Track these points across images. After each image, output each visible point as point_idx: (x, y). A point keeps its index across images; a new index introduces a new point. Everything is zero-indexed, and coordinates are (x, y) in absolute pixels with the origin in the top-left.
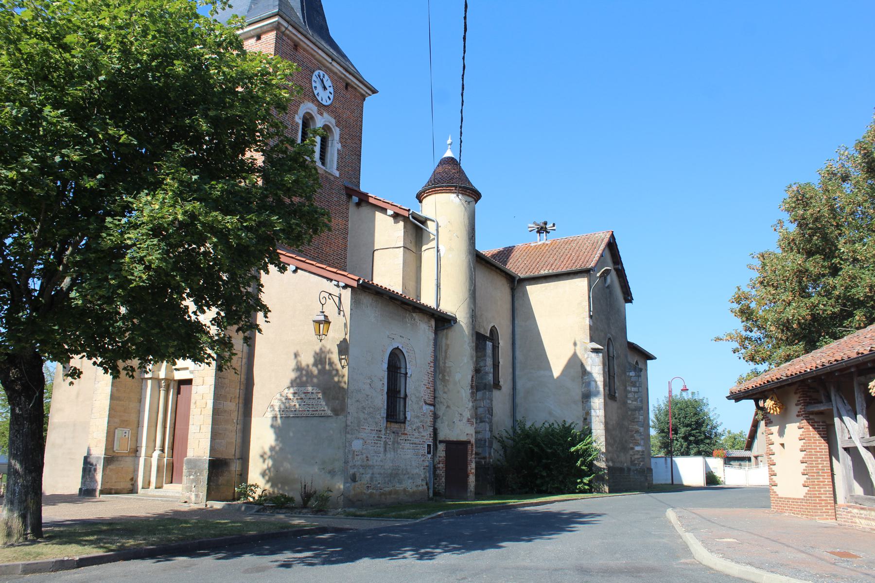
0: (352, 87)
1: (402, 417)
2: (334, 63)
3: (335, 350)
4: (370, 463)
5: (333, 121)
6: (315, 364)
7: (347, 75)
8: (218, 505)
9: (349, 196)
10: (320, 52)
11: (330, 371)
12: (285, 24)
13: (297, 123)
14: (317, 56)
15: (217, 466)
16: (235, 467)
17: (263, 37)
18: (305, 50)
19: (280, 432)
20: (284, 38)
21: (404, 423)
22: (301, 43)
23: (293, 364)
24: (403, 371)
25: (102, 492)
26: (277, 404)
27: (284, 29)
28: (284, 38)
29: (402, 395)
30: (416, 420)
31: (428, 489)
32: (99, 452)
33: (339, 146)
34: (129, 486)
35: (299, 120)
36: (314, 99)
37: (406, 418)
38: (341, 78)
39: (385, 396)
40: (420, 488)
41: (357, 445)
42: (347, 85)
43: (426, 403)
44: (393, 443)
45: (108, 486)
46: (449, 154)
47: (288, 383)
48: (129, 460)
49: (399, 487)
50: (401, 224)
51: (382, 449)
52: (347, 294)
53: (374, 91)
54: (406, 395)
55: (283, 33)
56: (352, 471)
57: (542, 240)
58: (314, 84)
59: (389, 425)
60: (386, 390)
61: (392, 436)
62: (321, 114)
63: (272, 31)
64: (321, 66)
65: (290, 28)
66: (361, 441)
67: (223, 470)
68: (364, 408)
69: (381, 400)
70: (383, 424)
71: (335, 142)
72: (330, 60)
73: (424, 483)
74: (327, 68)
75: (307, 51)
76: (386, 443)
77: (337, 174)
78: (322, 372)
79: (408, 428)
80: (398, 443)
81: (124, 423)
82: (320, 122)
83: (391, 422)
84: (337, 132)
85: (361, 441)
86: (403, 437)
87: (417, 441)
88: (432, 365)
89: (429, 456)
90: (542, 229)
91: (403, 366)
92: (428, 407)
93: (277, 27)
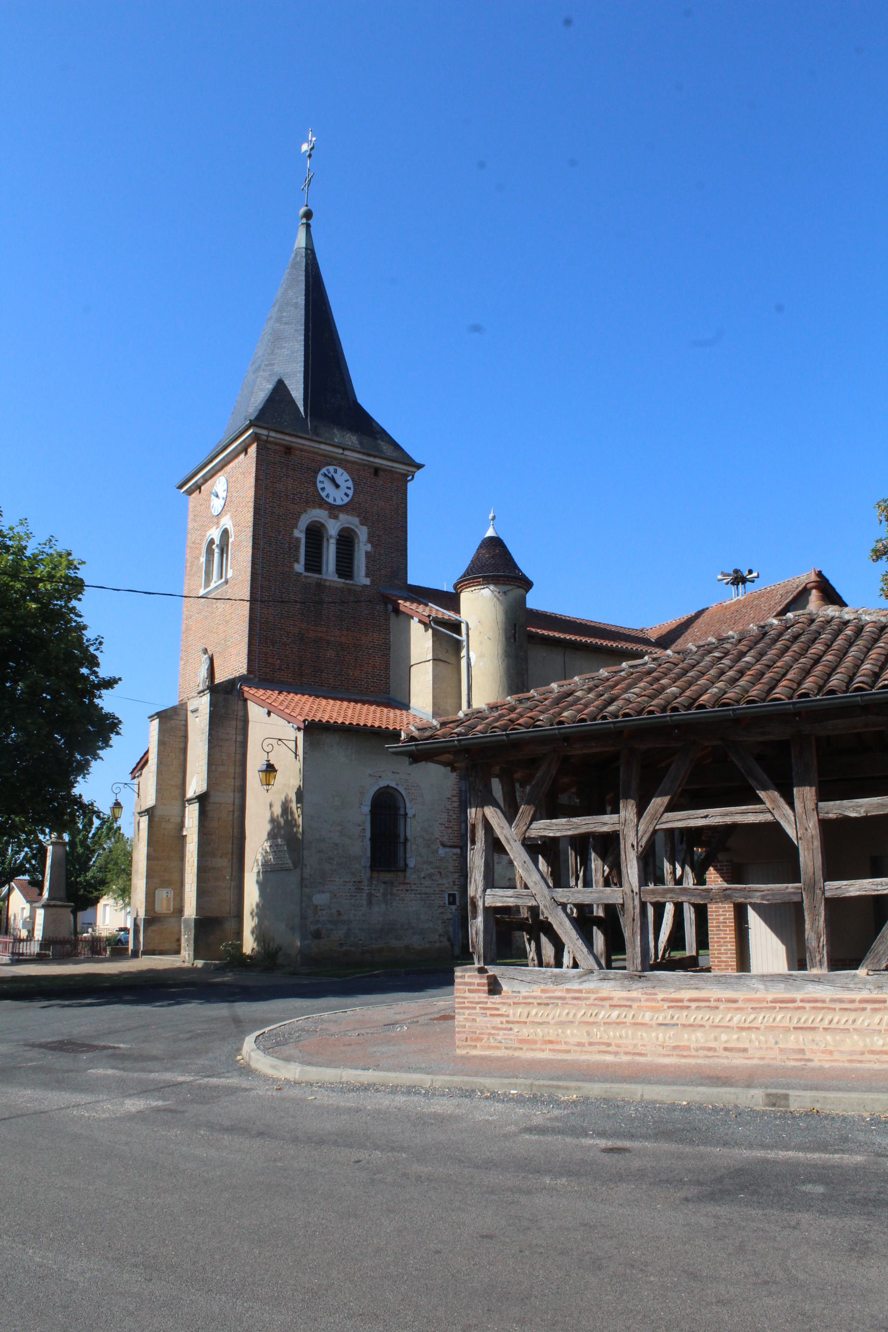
0: (385, 470)
1: (402, 864)
2: (347, 453)
3: (294, 799)
4: (345, 918)
5: (356, 520)
6: (282, 815)
7: (371, 459)
8: (200, 963)
9: (386, 604)
10: (323, 446)
11: (291, 821)
12: (265, 432)
13: (298, 540)
14: (321, 452)
15: (206, 925)
16: (230, 926)
17: (249, 450)
18: (302, 450)
19: (262, 886)
20: (269, 446)
21: (405, 871)
22: (293, 445)
23: (268, 816)
24: (402, 812)
25: (145, 953)
26: (260, 857)
27: (265, 438)
28: (269, 446)
29: (402, 839)
30: (425, 866)
31: (452, 945)
32: (142, 915)
33: (369, 547)
34: (175, 946)
35: (299, 534)
36: (322, 503)
37: (406, 865)
38: (365, 465)
39: (369, 843)
40: (437, 945)
41: (320, 899)
42: (377, 471)
43: (444, 845)
44: (385, 895)
45: (150, 947)
46: (490, 533)
47: (265, 836)
48: (174, 920)
49: (394, 943)
50: (430, 631)
51: (364, 902)
52: (300, 735)
53: (419, 466)
54: (406, 840)
55: (267, 441)
56: (313, 928)
57: (736, 595)
58: (320, 486)
59: (375, 875)
60: (368, 834)
61: (382, 888)
62: (336, 517)
63: (253, 443)
64: (330, 460)
65: (273, 434)
66: (328, 895)
67: (214, 926)
68: (332, 859)
69: (360, 846)
70: (366, 874)
71: (361, 544)
72: (341, 451)
73: (444, 939)
74: (341, 459)
75: (305, 451)
76: (370, 896)
77: (367, 581)
78: (286, 821)
79: (411, 877)
80: (392, 894)
81: (165, 884)
82: (333, 528)
83: (378, 871)
84: (362, 533)
85: (328, 895)
86: (402, 887)
87: (428, 890)
88: (455, 799)
89: (453, 907)
90: (739, 579)
91: (402, 805)
92: (448, 850)
93: (256, 438)
